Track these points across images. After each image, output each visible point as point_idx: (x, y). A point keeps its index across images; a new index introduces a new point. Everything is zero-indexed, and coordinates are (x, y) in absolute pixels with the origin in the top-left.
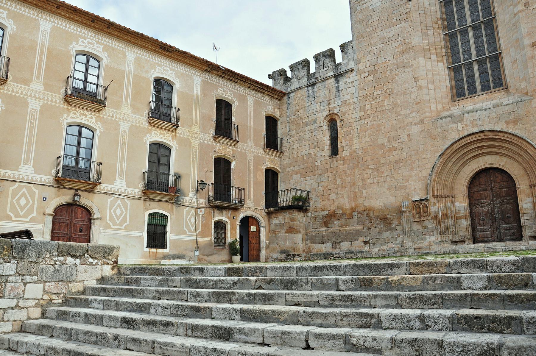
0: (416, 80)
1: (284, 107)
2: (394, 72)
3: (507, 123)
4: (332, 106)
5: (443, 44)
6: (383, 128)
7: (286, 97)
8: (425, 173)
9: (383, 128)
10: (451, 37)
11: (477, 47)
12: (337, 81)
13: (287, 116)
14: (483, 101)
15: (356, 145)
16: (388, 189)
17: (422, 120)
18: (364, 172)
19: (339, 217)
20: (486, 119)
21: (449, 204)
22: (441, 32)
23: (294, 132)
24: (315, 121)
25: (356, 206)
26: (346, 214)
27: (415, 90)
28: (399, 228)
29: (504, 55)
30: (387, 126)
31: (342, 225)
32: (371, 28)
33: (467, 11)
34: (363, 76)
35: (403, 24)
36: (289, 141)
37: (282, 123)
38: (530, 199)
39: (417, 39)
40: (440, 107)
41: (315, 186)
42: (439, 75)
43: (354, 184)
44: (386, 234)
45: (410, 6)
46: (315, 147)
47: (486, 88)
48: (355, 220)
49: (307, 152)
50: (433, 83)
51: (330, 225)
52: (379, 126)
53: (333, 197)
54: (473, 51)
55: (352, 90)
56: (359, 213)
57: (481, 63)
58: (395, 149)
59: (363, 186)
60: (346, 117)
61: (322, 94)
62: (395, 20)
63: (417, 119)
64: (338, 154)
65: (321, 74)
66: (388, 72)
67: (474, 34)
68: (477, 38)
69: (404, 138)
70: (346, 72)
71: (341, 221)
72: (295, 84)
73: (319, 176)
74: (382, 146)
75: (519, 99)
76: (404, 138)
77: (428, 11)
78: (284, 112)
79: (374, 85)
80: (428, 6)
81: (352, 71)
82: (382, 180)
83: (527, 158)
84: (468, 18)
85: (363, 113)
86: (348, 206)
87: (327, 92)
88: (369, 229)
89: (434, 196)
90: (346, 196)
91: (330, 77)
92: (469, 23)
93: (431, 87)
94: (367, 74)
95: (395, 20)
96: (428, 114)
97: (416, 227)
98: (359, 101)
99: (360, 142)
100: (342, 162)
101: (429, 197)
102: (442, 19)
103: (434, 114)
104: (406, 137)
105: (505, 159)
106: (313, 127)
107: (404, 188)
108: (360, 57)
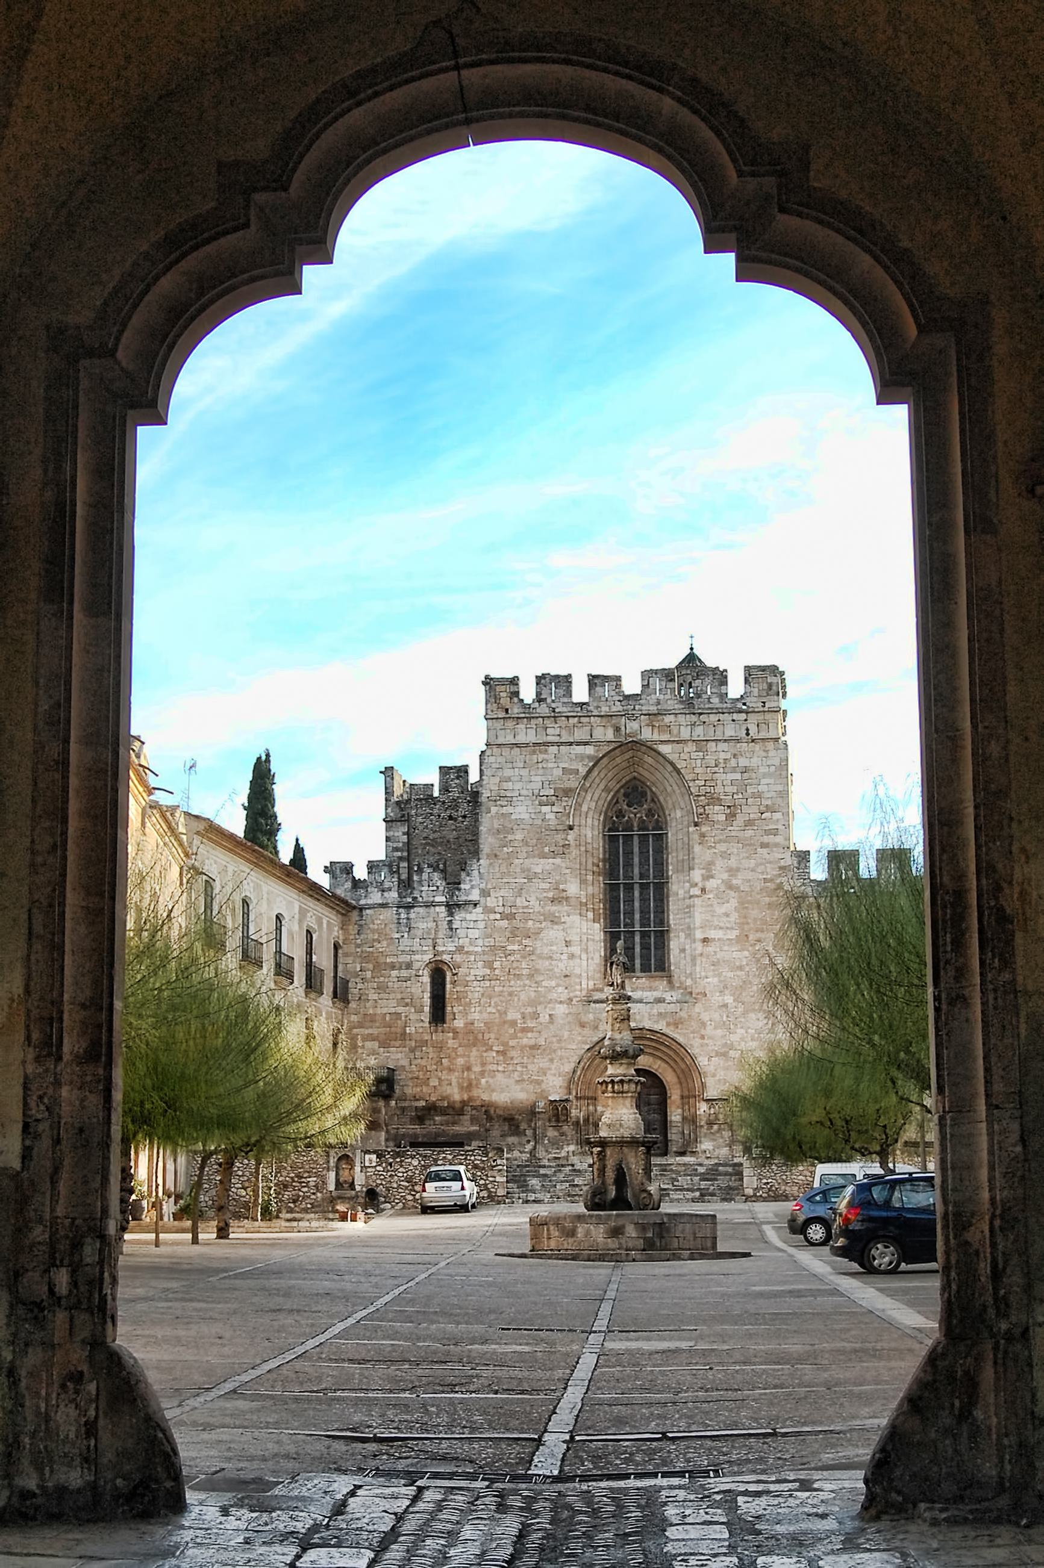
0: (568, 944)
1: (353, 929)
2: (538, 925)
3: (668, 1024)
4: (440, 949)
5: (601, 896)
6: (516, 999)
7: (355, 915)
8: (568, 1067)
9: (516, 999)
10: (612, 890)
11: (641, 912)
12: (451, 914)
13: (358, 946)
14: (643, 989)
15: (475, 1015)
16: (517, 1082)
17: (571, 1000)
18: (485, 1054)
19: (443, 1111)
20: (647, 1015)
21: (591, 1108)
22: (601, 878)
23: (369, 974)
24: (409, 966)
25: (470, 1099)
26: (453, 1108)
27: (565, 957)
28: (529, 1132)
29: (672, 935)
30: (522, 997)
31: (447, 1123)
32: (511, 849)
33: (636, 860)
34: (492, 916)
35: (558, 861)
36: (359, 986)
37: (346, 955)
38: (680, 1111)
39: (573, 888)
40: (591, 983)
41: (405, 1062)
42: (593, 940)
43: (469, 1069)
44: (511, 1140)
45: (569, 837)
46: (407, 1005)
47: (646, 968)
48: (467, 1117)
49: (393, 1010)
50: (586, 951)
51: (427, 1122)
52: (511, 994)
53: (434, 1082)
54: (637, 916)
55: (474, 934)
56: (474, 1108)
57: (644, 935)
58: (531, 1030)
59: (482, 1073)
60: (462, 971)
61: (422, 925)
62: (546, 849)
63: (564, 997)
64: (443, 1021)
65: (423, 894)
66: (530, 923)
67: (641, 894)
68: (644, 900)
69: (544, 1018)
70: (467, 903)
71: (445, 1118)
72: (376, 897)
73: (412, 1050)
74: (513, 1023)
75: (684, 999)
76: (544, 1018)
77: (590, 847)
78: (352, 937)
79: (508, 934)
80: (589, 841)
81: (475, 905)
82: (511, 1068)
83: (683, 1066)
84: (636, 871)
85: (488, 971)
86: (457, 1097)
87: (432, 925)
88: (487, 1130)
89: (577, 1098)
90: (454, 1083)
91: (439, 904)
92: (637, 879)
93: (584, 956)
94: (498, 916)
95: (546, 849)
96: (578, 993)
97: (551, 1133)
98: (484, 953)
99: (480, 1012)
100: (451, 1035)
101: (571, 1097)
102: (604, 860)
103: (584, 993)
104: (547, 1017)
105: (659, 1062)
106: (404, 973)
107: (539, 1083)
108: (489, 886)
